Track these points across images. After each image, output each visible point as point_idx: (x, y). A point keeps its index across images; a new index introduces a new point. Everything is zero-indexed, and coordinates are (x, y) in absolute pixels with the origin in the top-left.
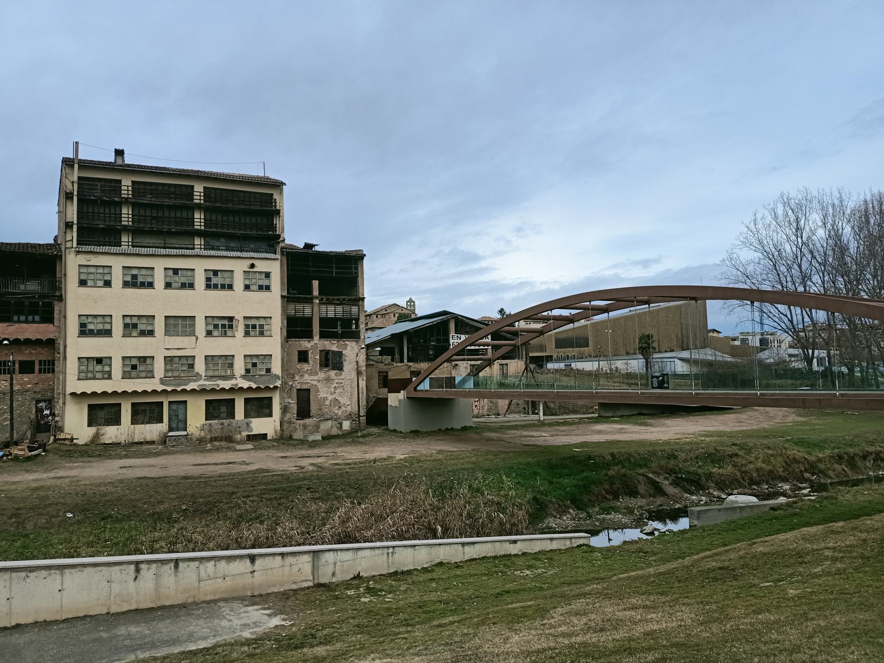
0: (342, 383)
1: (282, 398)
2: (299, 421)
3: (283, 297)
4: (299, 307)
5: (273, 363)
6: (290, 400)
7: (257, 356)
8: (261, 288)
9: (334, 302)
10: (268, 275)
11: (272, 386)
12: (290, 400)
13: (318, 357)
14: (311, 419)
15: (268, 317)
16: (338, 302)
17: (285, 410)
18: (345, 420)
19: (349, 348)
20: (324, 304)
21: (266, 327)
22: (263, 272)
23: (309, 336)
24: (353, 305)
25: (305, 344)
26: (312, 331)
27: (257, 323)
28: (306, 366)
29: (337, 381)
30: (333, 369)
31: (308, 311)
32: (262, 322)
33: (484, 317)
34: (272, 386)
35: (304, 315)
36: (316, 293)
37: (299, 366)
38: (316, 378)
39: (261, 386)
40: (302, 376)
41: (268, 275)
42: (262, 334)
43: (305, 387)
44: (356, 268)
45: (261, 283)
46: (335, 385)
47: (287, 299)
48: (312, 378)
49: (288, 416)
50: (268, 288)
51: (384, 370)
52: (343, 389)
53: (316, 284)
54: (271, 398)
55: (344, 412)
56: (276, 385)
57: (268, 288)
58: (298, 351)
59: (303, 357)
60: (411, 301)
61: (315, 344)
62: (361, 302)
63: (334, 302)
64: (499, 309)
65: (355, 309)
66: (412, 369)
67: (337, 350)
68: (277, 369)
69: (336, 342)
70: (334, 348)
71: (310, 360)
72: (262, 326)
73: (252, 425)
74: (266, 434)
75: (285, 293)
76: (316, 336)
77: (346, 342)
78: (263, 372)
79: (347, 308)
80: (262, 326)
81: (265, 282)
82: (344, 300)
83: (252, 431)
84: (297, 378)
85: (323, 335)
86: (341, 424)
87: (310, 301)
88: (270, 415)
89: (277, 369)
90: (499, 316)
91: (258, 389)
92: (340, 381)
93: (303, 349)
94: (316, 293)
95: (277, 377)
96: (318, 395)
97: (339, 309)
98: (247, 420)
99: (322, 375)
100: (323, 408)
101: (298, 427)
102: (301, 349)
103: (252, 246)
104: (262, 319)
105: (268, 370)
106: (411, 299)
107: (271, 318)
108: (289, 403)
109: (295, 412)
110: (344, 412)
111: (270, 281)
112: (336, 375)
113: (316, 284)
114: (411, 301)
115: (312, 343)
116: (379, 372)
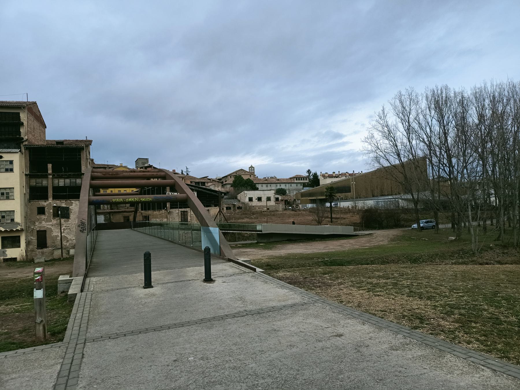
0: (69, 226)
1: (26, 236)
2: (39, 250)
3: (26, 175)
4: (39, 180)
5: (15, 216)
6: (32, 238)
7: (5, 212)
8: (7, 170)
9: (64, 176)
10: (11, 162)
11: (15, 230)
12: (32, 238)
13: (52, 211)
14: (47, 249)
15: (12, 188)
16: (66, 176)
17: (28, 243)
18: (70, 249)
19: (74, 205)
20: (56, 178)
21: (10, 194)
22: (8, 161)
23: (45, 198)
24: (77, 178)
25: (43, 203)
26: (47, 195)
27: (5, 192)
28: (43, 217)
29: (65, 225)
30: (63, 217)
31: (45, 183)
32: (8, 191)
33: (297, 175)
34: (15, 230)
35: (42, 185)
36: (50, 171)
37: (38, 217)
38: (51, 223)
39: (7, 230)
40: (41, 223)
41: (11, 162)
42: (8, 198)
43: (42, 229)
44: (80, 155)
45: (7, 167)
46: (64, 228)
47: (29, 176)
48: (48, 223)
49: (31, 247)
50: (12, 170)
51: (127, 216)
52: (70, 230)
53: (50, 166)
54: (19, 236)
55: (71, 244)
56: (17, 229)
57: (12, 170)
58: (38, 207)
59: (41, 211)
60: (252, 167)
61: (50, 203)
62: (82, 176)
63: (64, 176)
64: (307, 170)
65: (78, 181)
66: (144, 215)
67: (65, 206)
68: (18, 218)
69: (64, 201)
70: (64, 205)
71: (46, 212)
72: (7, 193)
73: (7, 253)
74: (16, 259)
75: (28, 173)
76: (50, 198)
77: (72, 201)
78: (9, 221)
79: (73, 180)
80: (7, 193)
81: (9, 167)
82: (70, 175)
83: (7, 256)
84: (37, 224)
85: (55, 198)
86: (69, 251)
87: (46, 177)
88: (19, 247)
89: (18, 218)
90: (308, 174)
91: (6, 231)
92: (67, 225)
93: (41, 206)
94: (50, 171)
95: (19, 224)
96: (52, 234)
97: (68, 181)
98: (3, 250)
99: (54, 222)
100: (56, 241)
101: (38, 253)
102: (39, 206)
103: (6, 145)
104: (8, 189)
105: (13, 220)
106: (252, 166)
107: (13, 188)
108: (32, 239)
109: (36, 244)
110: (71, 244)
111: (13, 166)
112: (65, 221)
113: (50, 166)
114: (252, 167)
115: (48, 203)
116: (124, 217)
